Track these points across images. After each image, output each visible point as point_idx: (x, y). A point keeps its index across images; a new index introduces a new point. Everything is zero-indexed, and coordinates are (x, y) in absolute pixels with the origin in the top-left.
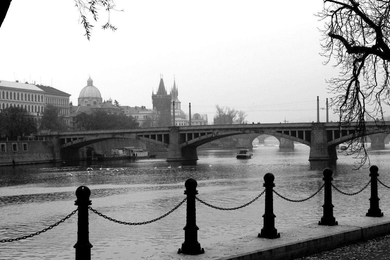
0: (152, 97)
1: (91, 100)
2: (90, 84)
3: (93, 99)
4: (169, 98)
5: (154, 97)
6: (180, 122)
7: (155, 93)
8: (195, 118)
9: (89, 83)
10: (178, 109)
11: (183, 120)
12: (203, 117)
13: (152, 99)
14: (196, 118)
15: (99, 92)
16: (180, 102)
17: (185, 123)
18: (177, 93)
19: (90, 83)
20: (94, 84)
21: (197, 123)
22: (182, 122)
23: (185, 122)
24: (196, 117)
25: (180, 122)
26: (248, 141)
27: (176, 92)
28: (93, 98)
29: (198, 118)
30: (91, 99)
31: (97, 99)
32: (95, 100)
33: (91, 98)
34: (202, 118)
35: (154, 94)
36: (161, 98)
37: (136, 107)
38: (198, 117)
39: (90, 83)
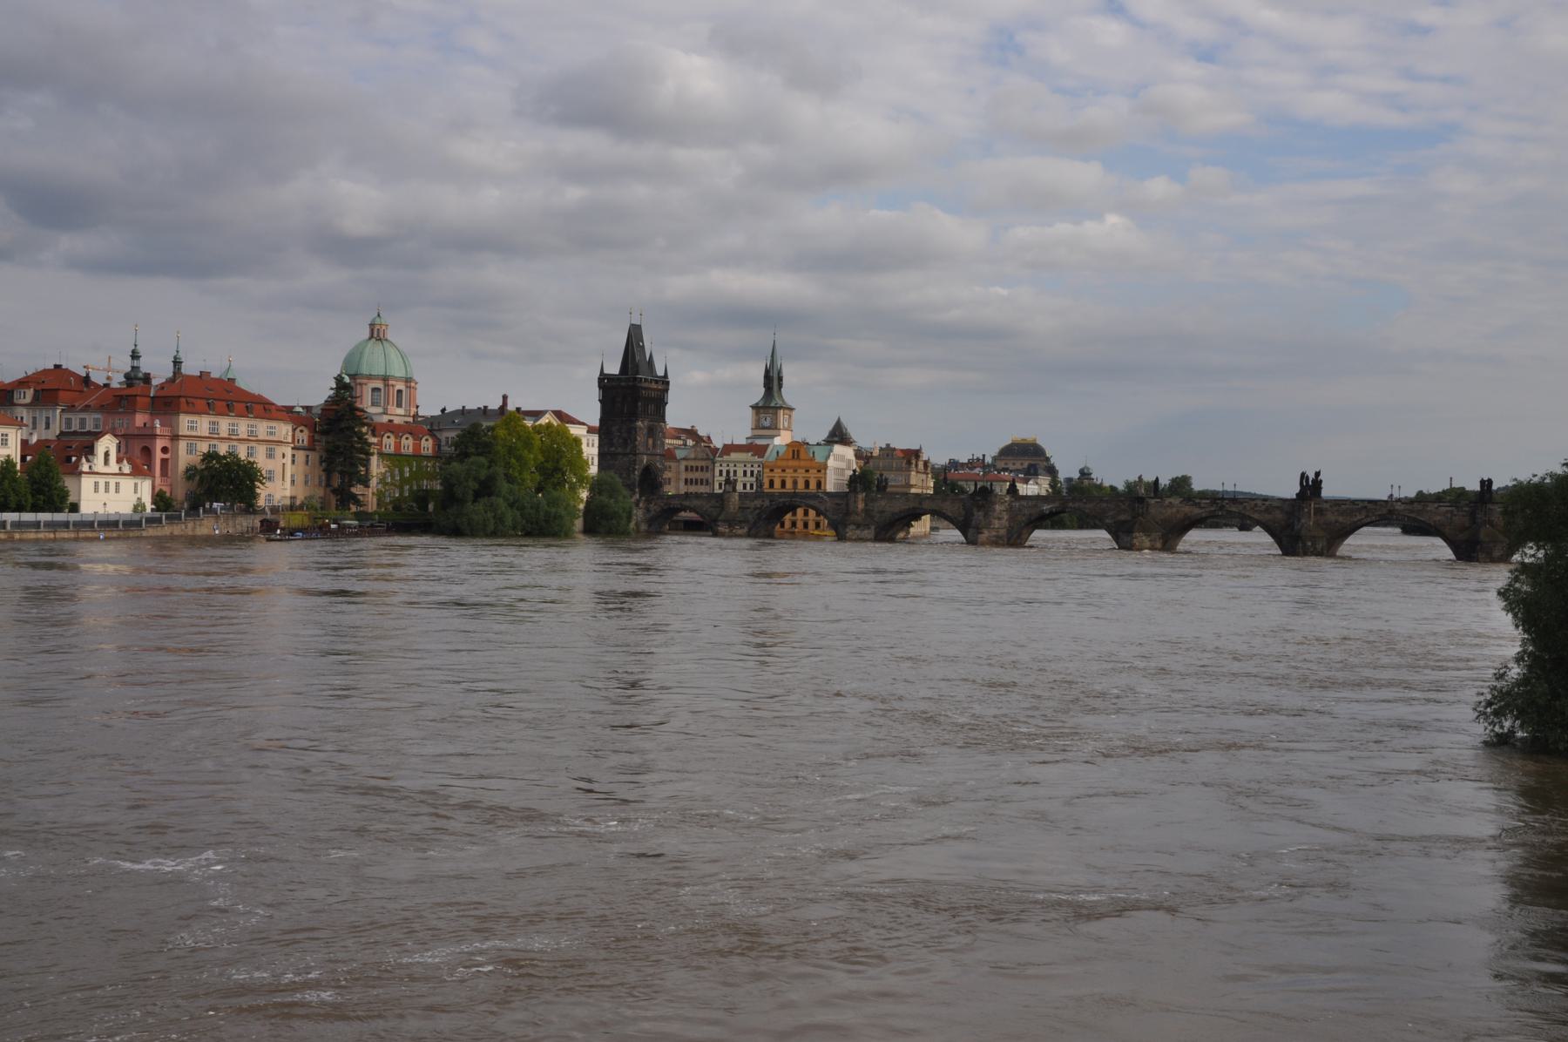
0: (601, 380)
4: (654, 386)
5: (605, 382)
6: (745, 466)
7: (614, 368)
12: (814, 453)
13: (600, 387)
14: (793, 457)
16: (791, 409)
17: (760, 469)
18: (780, 379)
21: (795, 471)
22: (752, 466)
23: (759, 466)
24: (794, 451)
25: (745, 466)
27: (775, 376)
29: (798, 456)
32: (379, 384)
34: (811, 455)
36: (623, 384)
37: (486, 407)
38: (798, 451)
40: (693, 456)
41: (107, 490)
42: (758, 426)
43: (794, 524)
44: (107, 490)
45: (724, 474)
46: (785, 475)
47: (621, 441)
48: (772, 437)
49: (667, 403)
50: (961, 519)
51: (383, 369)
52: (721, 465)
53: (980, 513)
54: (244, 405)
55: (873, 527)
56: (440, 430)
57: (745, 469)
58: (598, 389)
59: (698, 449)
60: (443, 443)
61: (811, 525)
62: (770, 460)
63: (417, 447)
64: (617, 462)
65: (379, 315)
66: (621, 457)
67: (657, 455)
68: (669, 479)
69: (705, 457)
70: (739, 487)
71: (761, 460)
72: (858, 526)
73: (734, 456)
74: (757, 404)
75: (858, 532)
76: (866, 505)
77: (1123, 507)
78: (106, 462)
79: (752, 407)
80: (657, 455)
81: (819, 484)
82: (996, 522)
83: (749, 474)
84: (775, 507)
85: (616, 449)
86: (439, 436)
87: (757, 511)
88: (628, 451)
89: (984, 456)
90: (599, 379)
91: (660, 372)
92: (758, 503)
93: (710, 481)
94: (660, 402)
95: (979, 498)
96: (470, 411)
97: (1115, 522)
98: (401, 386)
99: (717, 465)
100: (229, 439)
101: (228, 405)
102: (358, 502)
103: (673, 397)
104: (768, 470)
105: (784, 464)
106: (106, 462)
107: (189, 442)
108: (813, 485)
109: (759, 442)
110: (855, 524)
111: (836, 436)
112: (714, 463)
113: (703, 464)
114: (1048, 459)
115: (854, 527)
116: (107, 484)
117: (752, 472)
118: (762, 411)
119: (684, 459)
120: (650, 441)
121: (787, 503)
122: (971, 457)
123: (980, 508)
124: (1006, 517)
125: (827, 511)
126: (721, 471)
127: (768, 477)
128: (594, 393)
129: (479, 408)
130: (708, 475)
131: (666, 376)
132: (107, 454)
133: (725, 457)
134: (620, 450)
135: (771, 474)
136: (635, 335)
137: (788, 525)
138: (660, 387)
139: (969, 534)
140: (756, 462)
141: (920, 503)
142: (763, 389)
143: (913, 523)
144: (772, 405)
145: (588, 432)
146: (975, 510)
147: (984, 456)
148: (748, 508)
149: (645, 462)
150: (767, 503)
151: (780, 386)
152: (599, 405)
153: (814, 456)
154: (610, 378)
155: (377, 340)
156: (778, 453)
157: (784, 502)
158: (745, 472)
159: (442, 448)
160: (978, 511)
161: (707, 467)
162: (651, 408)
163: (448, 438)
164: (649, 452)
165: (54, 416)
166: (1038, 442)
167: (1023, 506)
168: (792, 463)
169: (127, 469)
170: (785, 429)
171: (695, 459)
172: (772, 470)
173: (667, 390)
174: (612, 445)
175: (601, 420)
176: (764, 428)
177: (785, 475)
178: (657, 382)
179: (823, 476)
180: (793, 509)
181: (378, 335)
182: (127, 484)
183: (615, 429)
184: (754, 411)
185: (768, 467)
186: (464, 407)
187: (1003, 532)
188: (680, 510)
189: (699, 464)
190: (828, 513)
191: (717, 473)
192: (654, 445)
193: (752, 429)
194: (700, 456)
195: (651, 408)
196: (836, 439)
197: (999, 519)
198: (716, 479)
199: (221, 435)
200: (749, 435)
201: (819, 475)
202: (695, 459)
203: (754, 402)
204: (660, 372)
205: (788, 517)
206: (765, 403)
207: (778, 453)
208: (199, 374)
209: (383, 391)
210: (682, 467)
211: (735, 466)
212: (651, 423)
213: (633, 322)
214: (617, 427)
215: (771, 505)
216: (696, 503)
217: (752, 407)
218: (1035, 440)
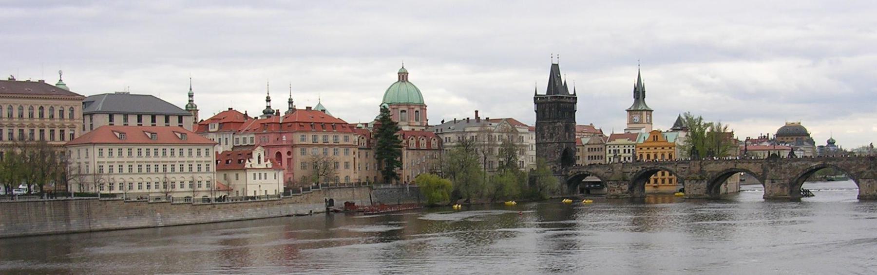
0: (535, 99)
1: (394, 108)
2: (401, 79)
3: (400, 105)
5: (539, 100)
6: (625, 147)
7: (543, 91)
8: (652, 139)
9: (399, 76)
10: (642, 123)
11: (631, 142)
12: (666, 137)
14: (654, 140)
15: (418, 91)
16: (651, 111)
17: (634, 148)
18: (644, 92)
19: (403, 76)
20: (410, 78)
21: (656, 148)
24: (654, 136)
26: (704, 185)
27: (641, 92)
28: (399, 105)
30: (394, 107)
31: (420, 106)
33: (394, 105)
34: (665, 139)
35: (538, 93)
36: (549, 100)
38: (657, 136)
39: (403, 76)
40: (592, 142)
41: (260, 178)
42: (631, 121)
43: (656, 181)
44: (260, 178)
45: (612, 152)
46: (649, 151)
47: (549, 135)
48: (640, 129)
49: (576, 111)
50: (760, 174)
51: (407, 100)
52: (610, 147)
53: (772, 170)
54: (330, 125)
55: (706, 181)
56: (442, 134)
57: (625, 148)
58: (534, 104)
59: (595, 138)
60: (444, 141)
61: (667, 181)
62: (640, 142)
63: (429, 143)
64: (547, 148)
65: (403, 68)
66: (549, 144)
67: (571, 143)
68: (579, 157)
69: (600, 142)
70: (622, 159)
71: (634, 142)
72: (697, 181)
73: (618, 141)
74: (630, 108)
75: (697, 184)
76: (701, 168)
77: (861, 163)
78: (259, 162)
79: (628, 111)
80: (571, 143)
81: (670, 156)
82: (783, 174)
83: (627, 151)
84: (644, 171)
85: (547, 140)
86: (442, 137)
87: (634, 174)
88: (553, 141)
89: (768, 134)
90: (534, 98)
91: (571, 92)
92: (634, 169)
93: (604, 157)
94: (572, 111)
95: (771, 161)
96: (459, 121)
97: (856, 173)
98: (417, 109)
99: (608, 147)
100: (323, 145)
101: (322, 126)
102: (398, 179)
103: (579, 106)
104: (639, 149)
105: (648, 144)
106: (259, 162)
107: (302, 148)
108: (667, 157)
109: (632, 132)
110: (695, 180)
111: (678, 126)
112: (606, 146)
113: (599, 146)
114: (808, 135)
115: (695, 182)
116: (260, 174)
117: (629, 150)
118: (633, 112)
119: (587, 144)
120: (567, 134)
121: (652, 169)
122: (760, 136)
123: (772, 167)
124: (788, 172)
125: (677, 172)
126: (610, 150)
127: (639, 153)
128: (532, 106)
129: (464, 119)
130: (603, 153)
131: (575, 94)
132: (259, 158)
133: (613, 142)
134: (548, 140)
135: (641, 151)
136: (555, 71)
137: (652, 181)
138: (571, 101)
139: (766, 184)
140: (631, 144)
141: (735, 166)
142: (634, 100)
143: (806, 186)
144: (639, 109)
145: (529, 130)
146: (769, 168)
147: (768, 134)
148: (629, 172)
149: (564, 147)
150: (640, 169)
151: (644, 97)
152: (535, 113)
153: (667, 139)
154: (542, 97)
155: (402, 82)
156: (644, 137)
157: (650, 168)
158: (625, 150)
159: (443, 144)
160: (772, 168)
161: (601, 148)
162: (567, 114)
163: (446, 138)
164: (566, 141)
165: (230, 137)
166: (801, 124)
167: (799, 165)
168: (655, 144)
169: (270, 166)
170: (648, 123)
171: (594, 144)
172: (641, 149)
173: (576, 103)
174: (543, 137)
175: (537, 123)
176: (635, 123)
177: (649, 151)
178: (569, 98)
179: (673, 151)
180: (655, 172)
181: (403, 79)
182: (270, 175)
183: (545, 127)
184: (629, 113)
185: (638, 147)
186: (455, 119)
187: (787, 181)
188: (585, 176)
189: (596, 146)
190: (678, 174)
191: (608, 152)
192: (569, 136)
193: (628, 124)
194: (596, 142)
195: (567, 114)
196: (679, 128)
197: (784, 173)
198: (607, 155)
199: (319, 143)
200: (626, 128)
201: (671, 150)
202: (594, 144)
203: (628, 108)
204: (571, 92)
205: (653, 176)
206: (635, 107)
207: (644, 137)
208: (305, 108)
209: (407, 112)
210: (586, 150)
211: (618, 147)
212: (567, 123)
213: (553, 63)
214: (547, 127)
215: (643, 170)
216: (595, 170)
217: (628, 111)
218: (800, 123)
